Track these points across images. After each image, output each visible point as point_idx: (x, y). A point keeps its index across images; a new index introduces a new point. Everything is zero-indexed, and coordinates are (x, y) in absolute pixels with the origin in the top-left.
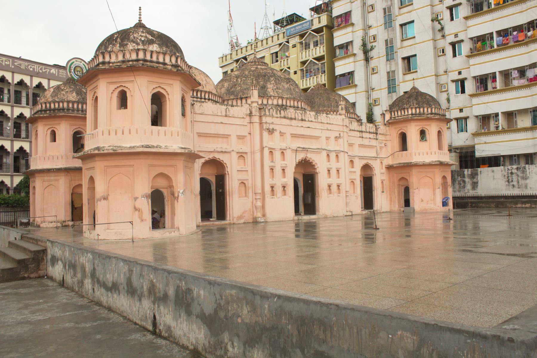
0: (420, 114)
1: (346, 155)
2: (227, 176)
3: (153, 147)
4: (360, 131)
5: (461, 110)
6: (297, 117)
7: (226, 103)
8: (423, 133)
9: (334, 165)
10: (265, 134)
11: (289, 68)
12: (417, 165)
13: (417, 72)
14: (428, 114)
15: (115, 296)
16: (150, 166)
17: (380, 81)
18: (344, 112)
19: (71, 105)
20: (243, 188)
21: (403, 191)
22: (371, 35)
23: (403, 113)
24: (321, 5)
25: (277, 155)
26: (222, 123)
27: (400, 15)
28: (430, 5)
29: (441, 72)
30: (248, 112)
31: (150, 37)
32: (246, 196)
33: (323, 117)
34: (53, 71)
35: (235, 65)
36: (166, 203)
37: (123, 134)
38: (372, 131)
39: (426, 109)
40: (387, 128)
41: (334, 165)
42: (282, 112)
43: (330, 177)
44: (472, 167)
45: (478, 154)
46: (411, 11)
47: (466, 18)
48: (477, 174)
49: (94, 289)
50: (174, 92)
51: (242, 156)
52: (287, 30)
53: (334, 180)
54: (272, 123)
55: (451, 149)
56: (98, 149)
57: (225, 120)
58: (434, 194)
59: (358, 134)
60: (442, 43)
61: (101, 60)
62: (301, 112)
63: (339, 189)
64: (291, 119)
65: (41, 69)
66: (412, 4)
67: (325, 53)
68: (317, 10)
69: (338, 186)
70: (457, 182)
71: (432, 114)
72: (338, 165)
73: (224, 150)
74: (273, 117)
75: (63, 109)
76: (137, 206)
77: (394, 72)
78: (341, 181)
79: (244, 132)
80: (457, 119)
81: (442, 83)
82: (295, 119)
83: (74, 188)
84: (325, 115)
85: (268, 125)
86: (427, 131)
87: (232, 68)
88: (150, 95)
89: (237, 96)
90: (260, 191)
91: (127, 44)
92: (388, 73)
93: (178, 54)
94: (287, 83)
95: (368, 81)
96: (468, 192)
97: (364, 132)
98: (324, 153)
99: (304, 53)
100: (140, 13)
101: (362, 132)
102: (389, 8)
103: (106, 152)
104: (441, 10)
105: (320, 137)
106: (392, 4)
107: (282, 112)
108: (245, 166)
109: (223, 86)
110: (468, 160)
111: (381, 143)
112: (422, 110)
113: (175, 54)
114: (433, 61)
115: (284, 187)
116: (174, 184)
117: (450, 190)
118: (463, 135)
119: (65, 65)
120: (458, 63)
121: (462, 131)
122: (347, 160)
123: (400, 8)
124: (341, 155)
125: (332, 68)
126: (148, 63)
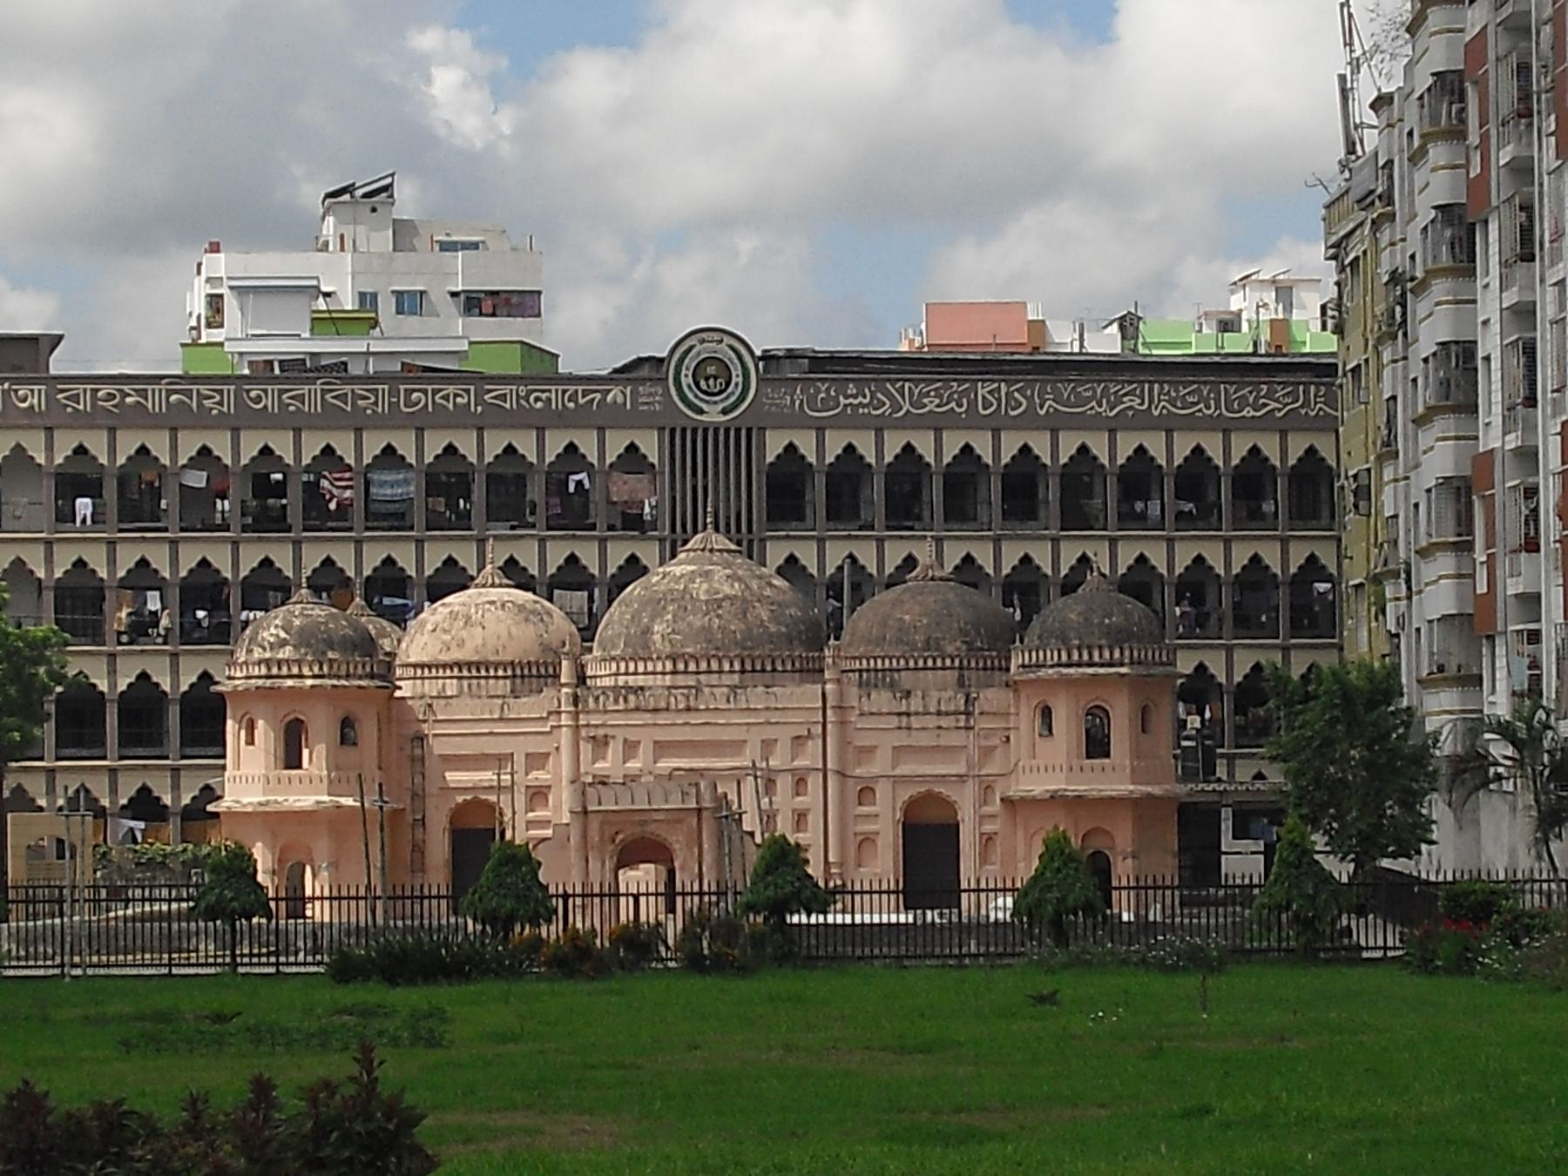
3: (276, 802)
10: (586, 749)
34: (615, 394)
38: (952, 708)
42: (632, 698)
59: (895, 721)
64: (656, 710)
71: (1059, 665)
74: (606, 712)
82: (667, 709)
84: (761, 689)
93: (330, 655)
97: (917, 714)
101: (908, 715)
105: (745, 741)
107: (632, 698)
111: (986, 738)
112: (1041, 654)
113: (324, 653)
124: (815, 782)
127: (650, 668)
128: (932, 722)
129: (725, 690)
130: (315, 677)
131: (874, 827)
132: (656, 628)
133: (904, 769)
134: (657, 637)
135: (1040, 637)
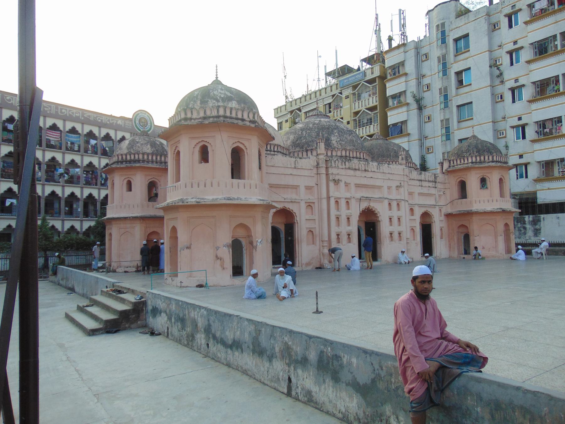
0: (480, 162)
1: (407, 203)
3: (234, 199)
4: (419, 180)
5: (521, 156)
6: (360, 168)
7: (292, 155)
8: (483, 181)
9: (395, 213)
10: (332, 184)
11: (342, 118)
12: (477, 213)
13: (472, 119)
14: (489, 162)
15: (237, 353)
17: (434, 129)
18: (404, 162)
19: (146, 157)
20: (311, 236)
21: (463, 238)
22: (424, 84)
23: (462, 161)
24: (374, 55)
25: (343, 203)
26: (291, 174)
27: (455, 62)
28: (489, 51)
29: (499, 118)
30: (316, 164)
31: (229, 94)
32: (313, 243)
33: (385, 167)
35: (289, 116)
36: (244, 252)
37: (205, 186)
38: (431, 179)
39: (486, 158)
40: (446, 177)
43: (391, 225)
44: (533, 214)
45: (540, 201)
46: (467, 58)
47: (529, 62)
48: (539, 221)
49: (208, 345)
50: (252, 147)
51: (310, 206)
52: (340, 81)
53: (396, 228)
54: (338, 174)
55: (513, 196)
56: (182, 200)
57: (295, 172)
58: (496, 242)
59: (418, 183)
60: (500, 89)
61: (183, 116)
62: (364, 163)
63: (400, 236)
64: (355, 169)
65: (109, 121)
66: (469, 51)
67: (378, 103)
68: (369, 60)
69: (400, 234)
70: (517, 229)
71: (493, 162)
73: (293, 201)
75: (139, 161)
76: (218, 256)
77: (448, 120)
78: (402, 228)
79: (312, 183)
80: (516, 166)
81: (499, 129)
83: (149, 235)
84: (386, 165)
85: (334, 176)
86: (488, 179)
87: (286, 119)
89: (302, 147)
90: (327, 239)
91: (208, 101)
92: (442, 121)
94: (350, 135)
96: (530, 239)
98: (386, 202)
99: (357, 104)
100: (217, 70)
101: (421, 181)
102: (444, 57)
103: (189, 204)
104: (500, 56)
106: (447, 51)
107: (347, 163)
108: (312, 214)
109: (289, 138)
110: (529, 206)
111: (440, 191)
113: (252, 110)
114: (490, 108)
115: (349, 235)
117: (512, 237)
118: (523, 181)
119: (131, 117)
120: (518, 108)
121: (522, 177)
122: (408, 210)
123: (455, 56)
124: (402, 204)
125: (385, 118)
126: (228, 119)
128: (427, 184)
130: (250, 121)
132: (333, 138)
133: (421, 202)
134: (334, 142)
135: (478, 151)
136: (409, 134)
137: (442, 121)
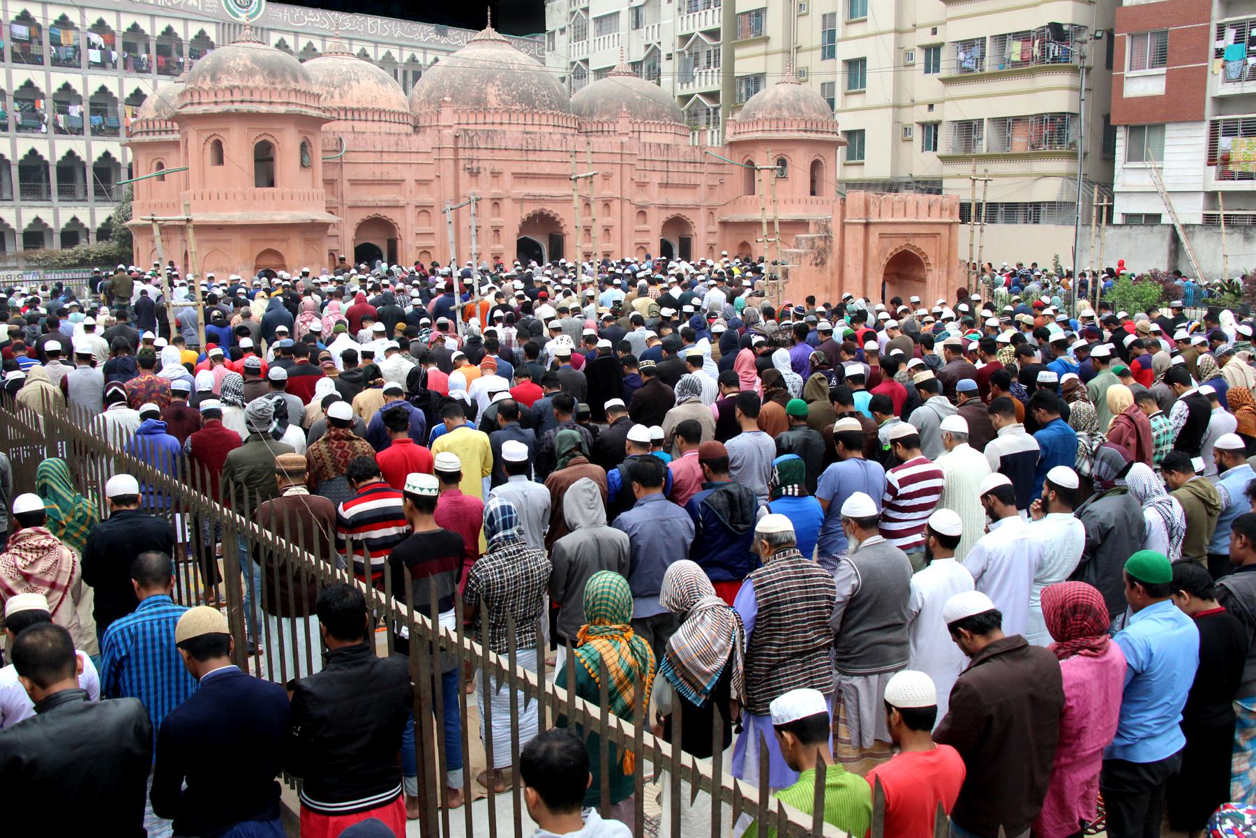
2: (399, 242)
5: (931, 107)
8: (782, 162)
10: (464, 176)
13: (865, 20)
16: (252, 241)
29: (907, 25)
40: (728, 149)
41: (600, 219)
72: (607, 221)
79: (428, 174)
86: (788, 161)
88: (253, 147)
95: (790, 30)
98: (577, 202)
116: (287, 263)
118: (931, 156)
124: (616, 206)
127: (489, 120)
129: (559, 136)
131: (646, 240)
136: (767, 39)
137: (824, 16)
